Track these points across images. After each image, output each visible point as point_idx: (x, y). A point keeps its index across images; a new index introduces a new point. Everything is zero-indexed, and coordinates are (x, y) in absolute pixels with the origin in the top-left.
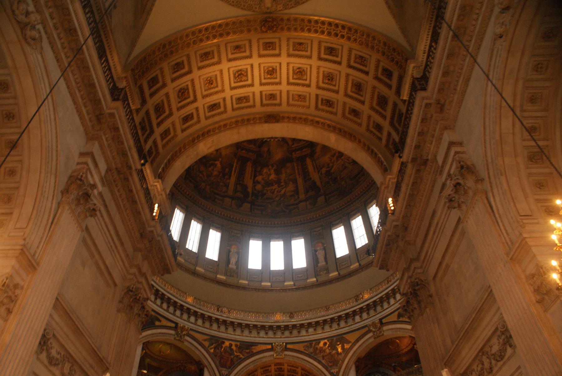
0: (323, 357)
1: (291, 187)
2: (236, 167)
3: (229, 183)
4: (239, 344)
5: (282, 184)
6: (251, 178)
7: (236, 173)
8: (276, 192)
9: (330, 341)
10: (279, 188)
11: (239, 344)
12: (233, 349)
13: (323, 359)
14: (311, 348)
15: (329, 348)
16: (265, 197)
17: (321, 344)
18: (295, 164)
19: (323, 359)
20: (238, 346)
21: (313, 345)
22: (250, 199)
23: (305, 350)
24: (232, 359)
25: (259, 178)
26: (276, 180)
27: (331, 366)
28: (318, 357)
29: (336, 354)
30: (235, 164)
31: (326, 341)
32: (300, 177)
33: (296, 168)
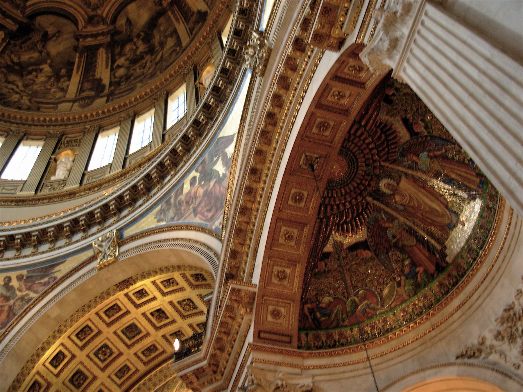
0: (195, 210)
1: (171, 42)
2: (80, 62)
3: (68, 86)
4: (24, 272)
5: (156, 50)
6: (107, 67)
7: (80, 71)
8: (148, 64)
9: (200, 168)
10: (153, 57)
11: (24, 272)
12: (12, 287)
13: (195, 215)
14: (169, 209)
15: (203, 183)
16: (132, 78)
17: (187, 187)
18: (169, 13)
19: (195, 215)
20: (25, 278)
21: (172, 200)
22: (106, 91)
23: (159, 221)
24: (10, 307)
25: (121, 61)
26: (146, 50)
27: (212, 217)
28: (185, 219)
29: (216, 185)
30: (77, 60)
31: (194, 174)
32: (179, 23)
33: (172, 17)
